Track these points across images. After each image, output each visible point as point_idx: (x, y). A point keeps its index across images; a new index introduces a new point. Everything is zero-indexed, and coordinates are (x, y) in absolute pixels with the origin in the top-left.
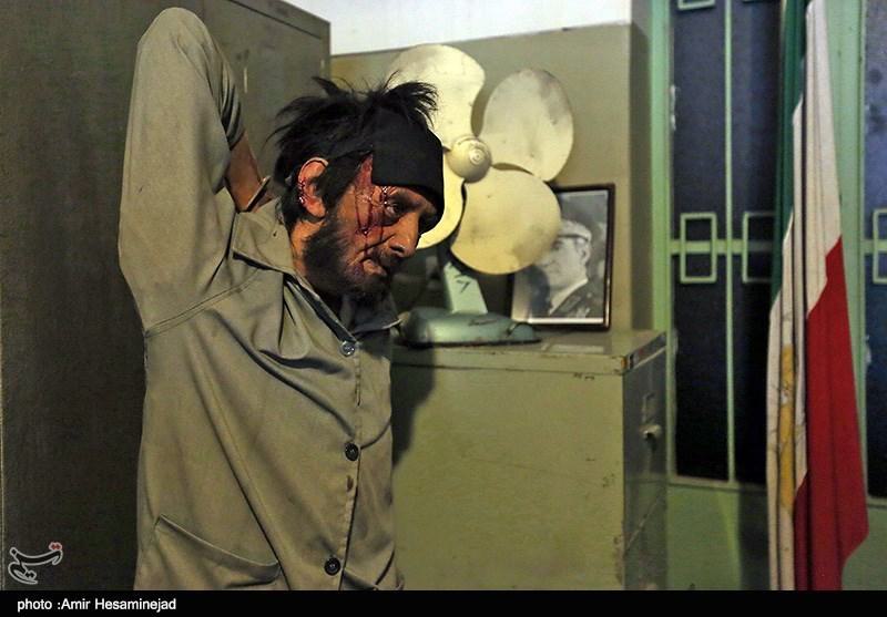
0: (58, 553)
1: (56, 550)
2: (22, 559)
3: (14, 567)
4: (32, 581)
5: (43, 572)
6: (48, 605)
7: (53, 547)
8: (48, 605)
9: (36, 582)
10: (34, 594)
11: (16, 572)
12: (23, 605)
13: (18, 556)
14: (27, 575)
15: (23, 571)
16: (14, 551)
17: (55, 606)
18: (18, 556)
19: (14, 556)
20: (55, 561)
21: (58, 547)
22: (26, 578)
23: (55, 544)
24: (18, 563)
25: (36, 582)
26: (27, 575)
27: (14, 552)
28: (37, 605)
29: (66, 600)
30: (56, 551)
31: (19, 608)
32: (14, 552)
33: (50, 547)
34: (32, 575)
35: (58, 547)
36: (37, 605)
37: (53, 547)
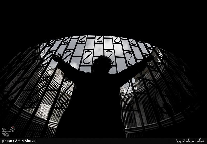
0: (13, 129)
1: (13, 128)
3: (3, 132)
4: (8, 136)
5: (10, 134)
6: (11, 141)
7: (12, 128)
8: (11, 141)
9: (8, 136)
10: (7, 138)
11: (4, 133)
13: (4, 130)
14: (6, 134)
15: (5, 133)
16: (3, 129)
17: (13, 141)
18: (4, 130)
19: (3, 130)
20: (13, 131)
21: (14, 128)
22: (6, 135)
23: (13, 127)
24: (5, 132)
25: (8, 136)
27: (3, 129)
29: (16, 140)
30: (13, 129)
31: (3, 142)
32: (3, 129)
33: (12, 128)
34: (7, 134)
35: (14, 128)
37: (12, 128)
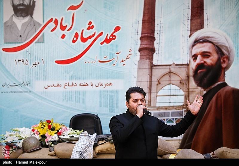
2: (5, 150)
3: (3, 153)
4: (8, 157)
6: (11, 163)
7: (14, 147)
8: (11, 163)
10: (7, 160)
11: (4, 154)
12: (4, 163)
14: (7, 155)
15: (6, 153)
17: (13, 163)
21: (15, 147)
24: (5, 152)
25: (9, 157)
26: (7, 155)
27: (3, 148)
28: (8, 163)
31: (3, 163)
32: (3, 148)
33: (13, 147)
34: (8, 155)
35: (15, 147)
36: (8, 163)
37: (14, 147)
